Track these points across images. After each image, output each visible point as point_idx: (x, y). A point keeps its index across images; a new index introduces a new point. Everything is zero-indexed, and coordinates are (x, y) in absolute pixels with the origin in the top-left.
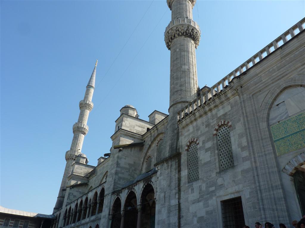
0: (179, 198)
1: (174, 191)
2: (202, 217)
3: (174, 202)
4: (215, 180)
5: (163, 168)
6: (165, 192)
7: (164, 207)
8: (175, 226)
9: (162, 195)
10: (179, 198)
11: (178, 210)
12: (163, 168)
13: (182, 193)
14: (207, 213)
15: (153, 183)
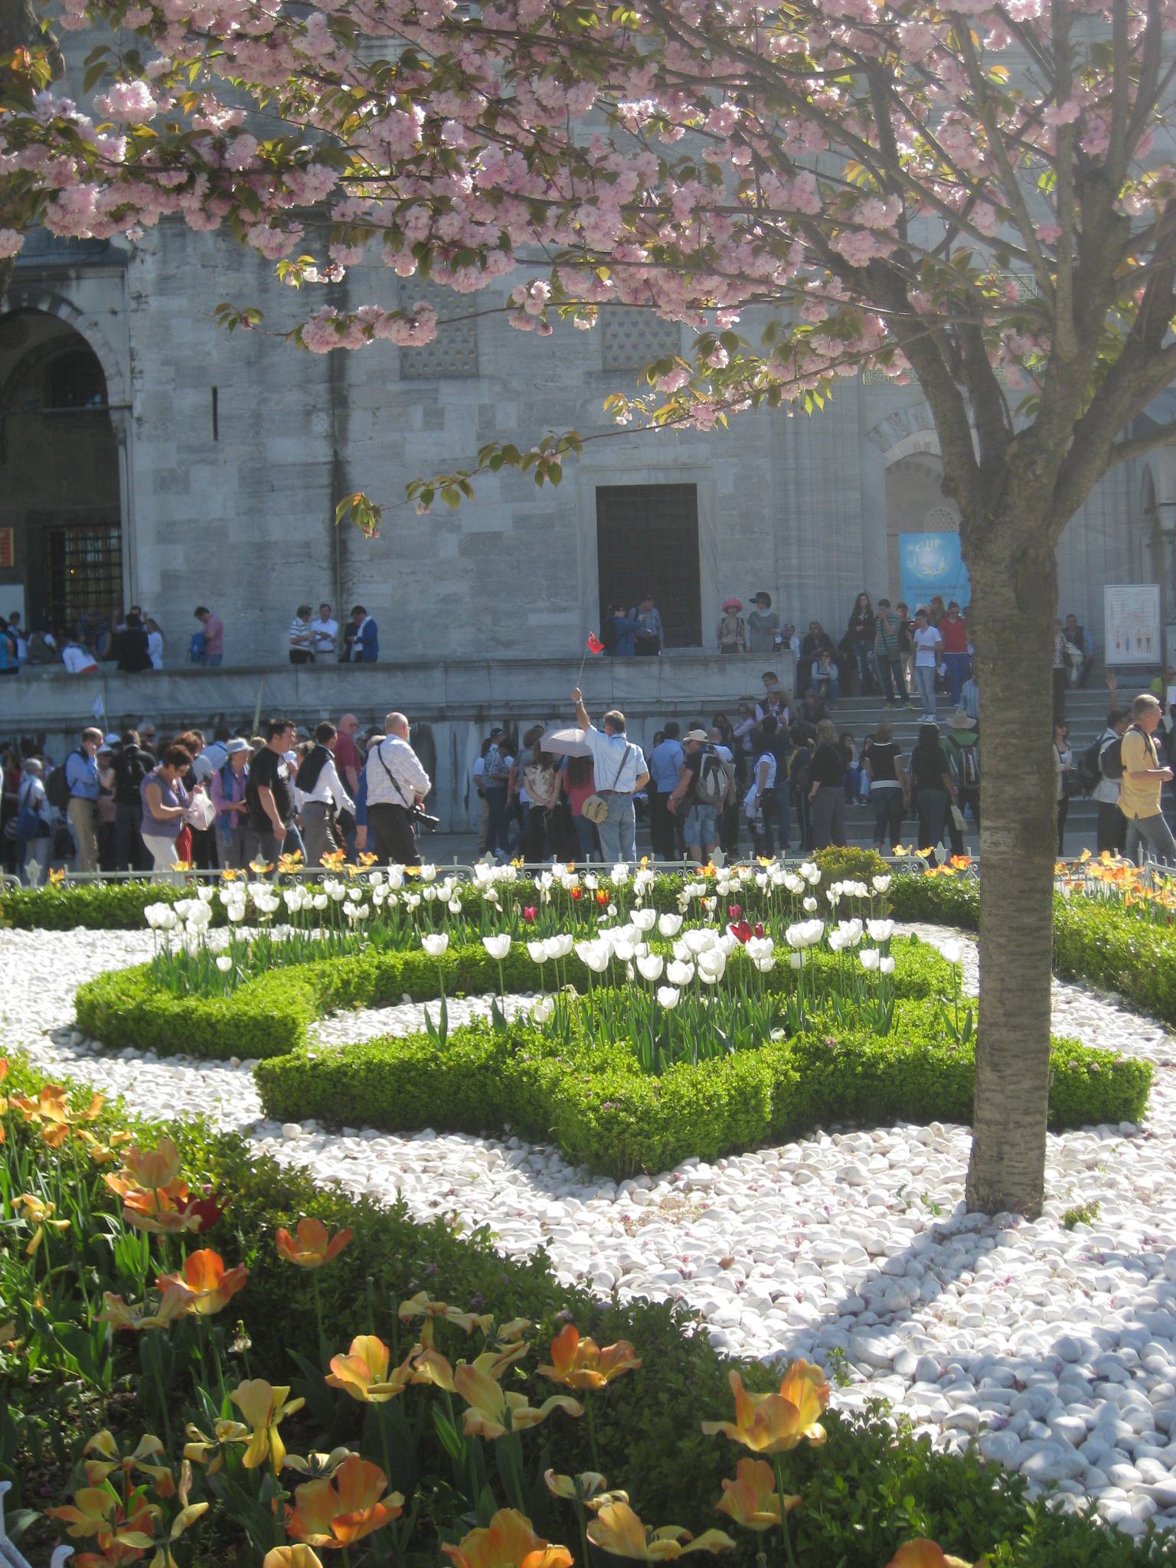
0: (338, 436)
1: (293, 399)
2: (496, 536)
3: (299, 448)
4: (579, 402)
5: (183, 249)
6: (215, 392)
7: (214, 462)
8: (309, 556)
9: (191, 400)
10: (338, 436)
11: (327, 491)
12: (190, 250)
13: (359, 422)
14: (521, 521)
15: (78, 312)
